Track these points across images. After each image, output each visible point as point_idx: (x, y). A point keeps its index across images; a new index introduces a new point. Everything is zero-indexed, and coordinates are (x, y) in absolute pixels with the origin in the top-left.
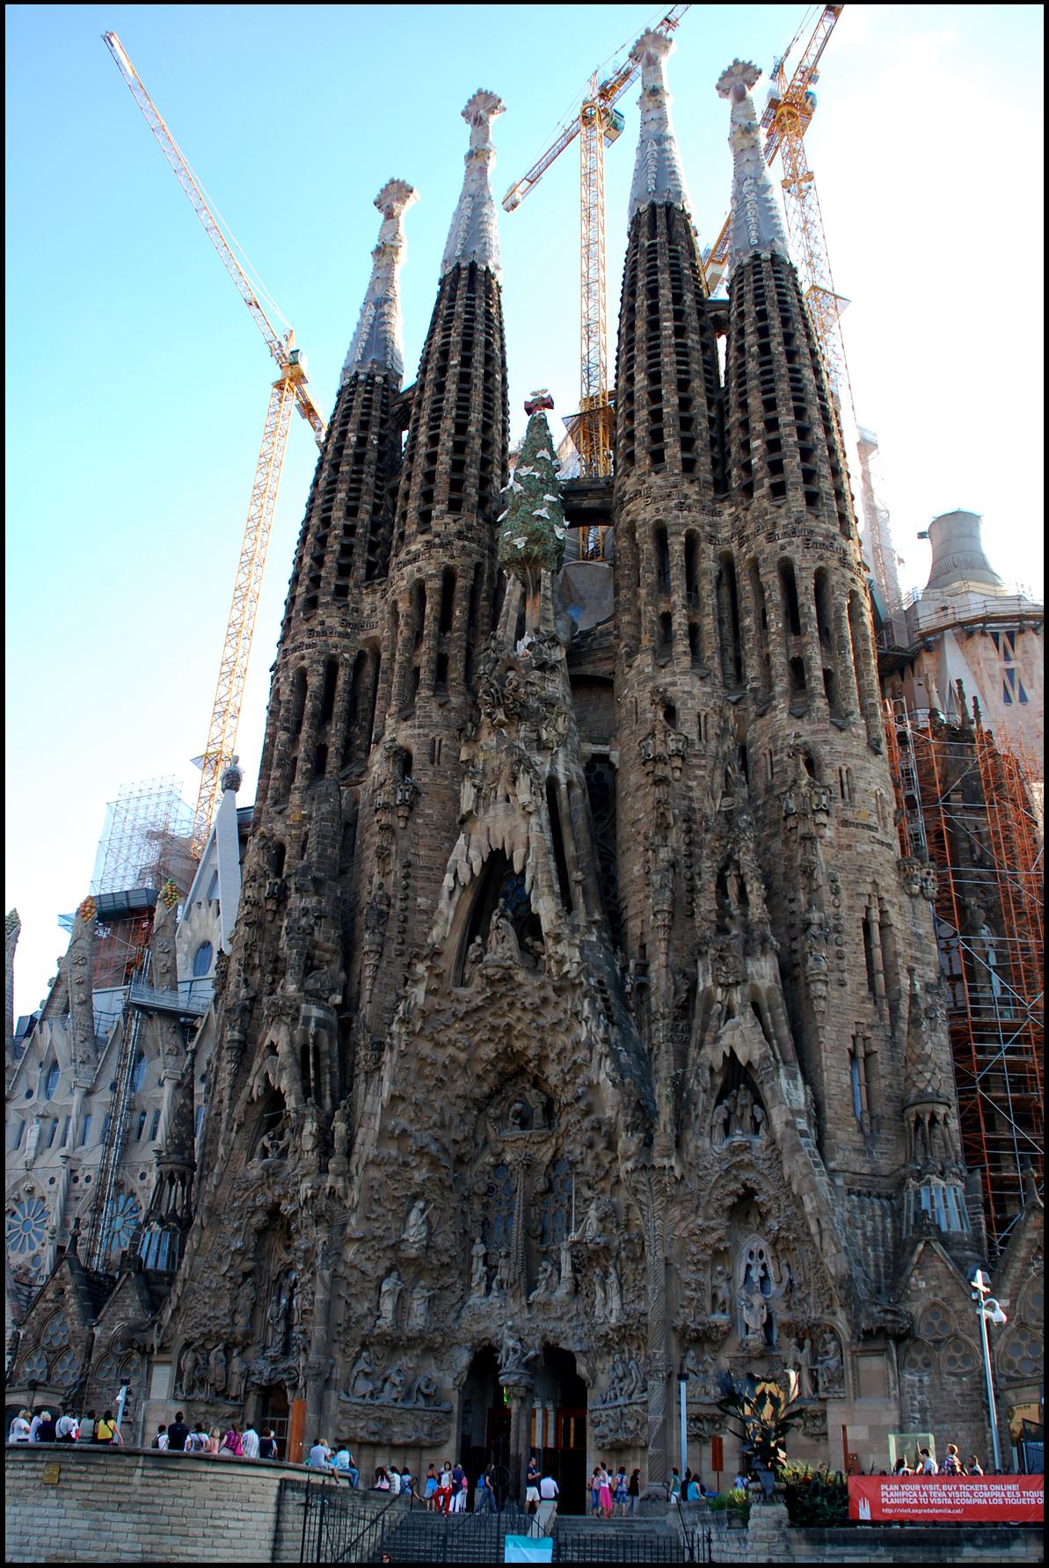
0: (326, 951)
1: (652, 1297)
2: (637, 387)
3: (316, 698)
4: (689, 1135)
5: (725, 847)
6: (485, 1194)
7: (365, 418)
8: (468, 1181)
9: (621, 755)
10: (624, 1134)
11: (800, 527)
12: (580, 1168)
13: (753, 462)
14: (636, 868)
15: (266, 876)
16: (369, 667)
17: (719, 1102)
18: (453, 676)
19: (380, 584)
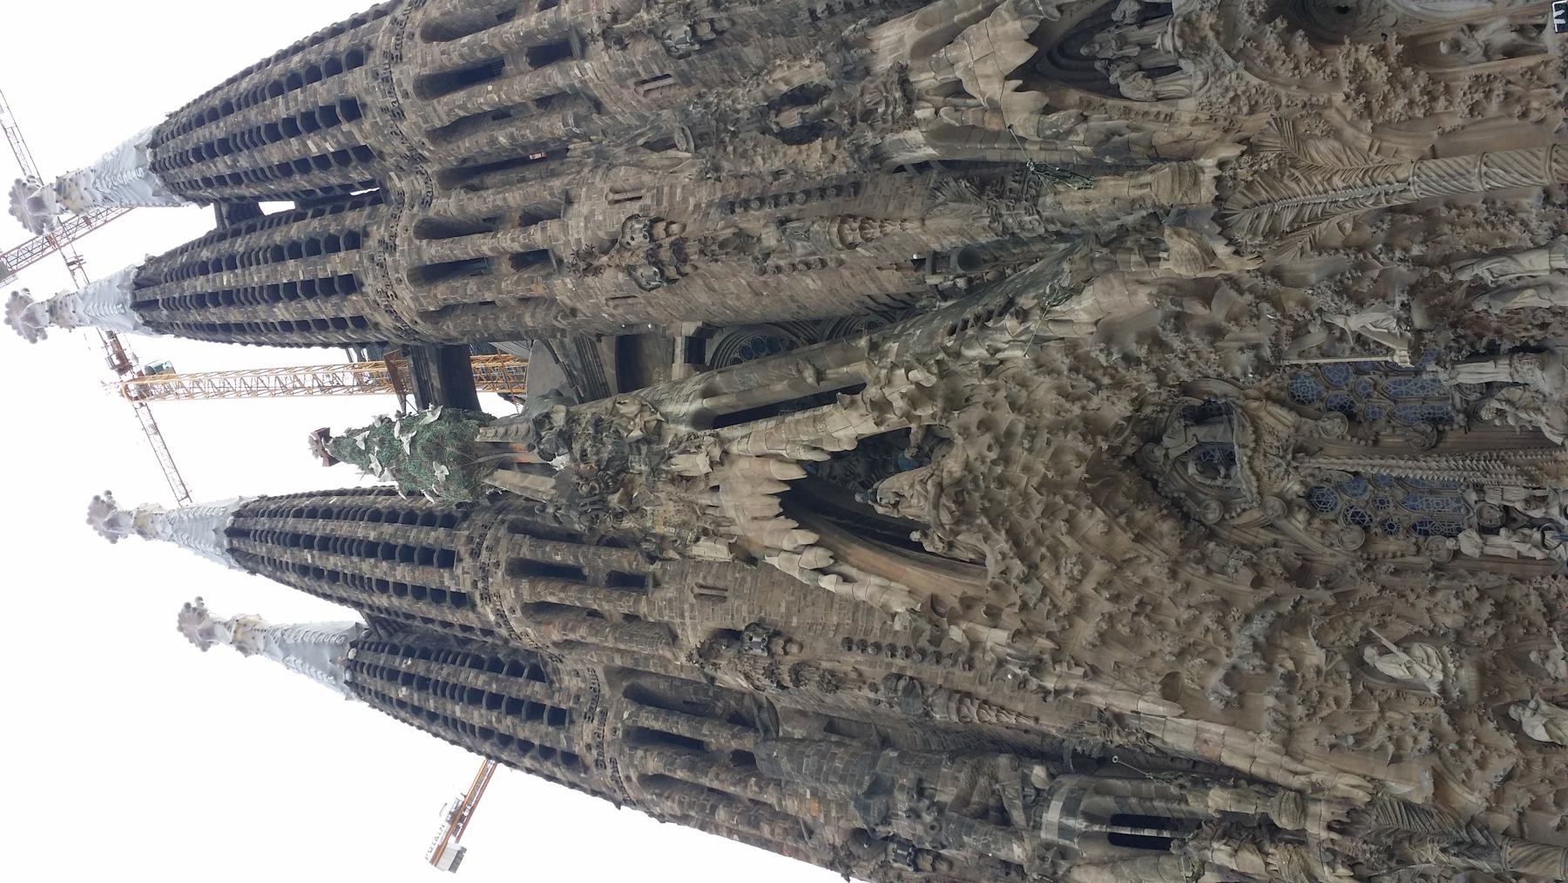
0: (973, 784)
1: (1500, 179)
2: (288, 317)
3: (672, 764)
4: (1162, 136)
5: (734, 135)
6: (1366, 529)
7: (385, 675)
8: (1341, 559)
9: (685, 319)
10: (1164, 266)
11: (381, 72)
12: (1267, 352)
13: (332, 150)
14: (812, 285)
15: (885, 865)
16: (646, 683)
17: (1115, 92)
18: (626, 565)
19: (546, 664)
